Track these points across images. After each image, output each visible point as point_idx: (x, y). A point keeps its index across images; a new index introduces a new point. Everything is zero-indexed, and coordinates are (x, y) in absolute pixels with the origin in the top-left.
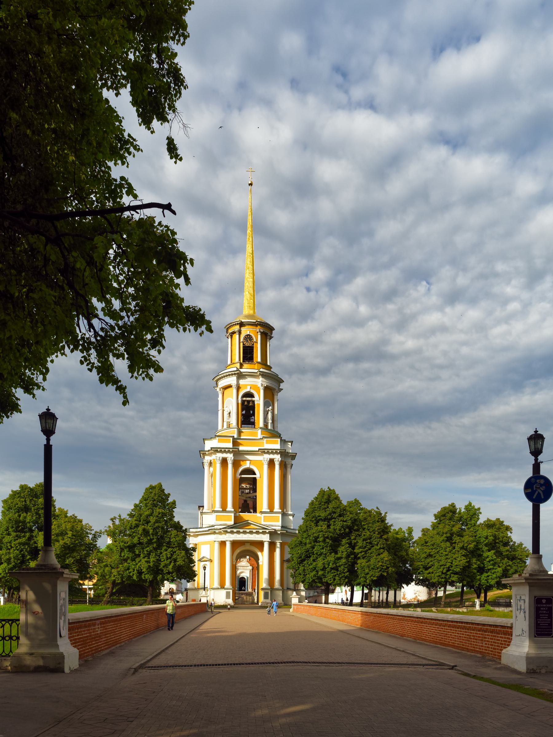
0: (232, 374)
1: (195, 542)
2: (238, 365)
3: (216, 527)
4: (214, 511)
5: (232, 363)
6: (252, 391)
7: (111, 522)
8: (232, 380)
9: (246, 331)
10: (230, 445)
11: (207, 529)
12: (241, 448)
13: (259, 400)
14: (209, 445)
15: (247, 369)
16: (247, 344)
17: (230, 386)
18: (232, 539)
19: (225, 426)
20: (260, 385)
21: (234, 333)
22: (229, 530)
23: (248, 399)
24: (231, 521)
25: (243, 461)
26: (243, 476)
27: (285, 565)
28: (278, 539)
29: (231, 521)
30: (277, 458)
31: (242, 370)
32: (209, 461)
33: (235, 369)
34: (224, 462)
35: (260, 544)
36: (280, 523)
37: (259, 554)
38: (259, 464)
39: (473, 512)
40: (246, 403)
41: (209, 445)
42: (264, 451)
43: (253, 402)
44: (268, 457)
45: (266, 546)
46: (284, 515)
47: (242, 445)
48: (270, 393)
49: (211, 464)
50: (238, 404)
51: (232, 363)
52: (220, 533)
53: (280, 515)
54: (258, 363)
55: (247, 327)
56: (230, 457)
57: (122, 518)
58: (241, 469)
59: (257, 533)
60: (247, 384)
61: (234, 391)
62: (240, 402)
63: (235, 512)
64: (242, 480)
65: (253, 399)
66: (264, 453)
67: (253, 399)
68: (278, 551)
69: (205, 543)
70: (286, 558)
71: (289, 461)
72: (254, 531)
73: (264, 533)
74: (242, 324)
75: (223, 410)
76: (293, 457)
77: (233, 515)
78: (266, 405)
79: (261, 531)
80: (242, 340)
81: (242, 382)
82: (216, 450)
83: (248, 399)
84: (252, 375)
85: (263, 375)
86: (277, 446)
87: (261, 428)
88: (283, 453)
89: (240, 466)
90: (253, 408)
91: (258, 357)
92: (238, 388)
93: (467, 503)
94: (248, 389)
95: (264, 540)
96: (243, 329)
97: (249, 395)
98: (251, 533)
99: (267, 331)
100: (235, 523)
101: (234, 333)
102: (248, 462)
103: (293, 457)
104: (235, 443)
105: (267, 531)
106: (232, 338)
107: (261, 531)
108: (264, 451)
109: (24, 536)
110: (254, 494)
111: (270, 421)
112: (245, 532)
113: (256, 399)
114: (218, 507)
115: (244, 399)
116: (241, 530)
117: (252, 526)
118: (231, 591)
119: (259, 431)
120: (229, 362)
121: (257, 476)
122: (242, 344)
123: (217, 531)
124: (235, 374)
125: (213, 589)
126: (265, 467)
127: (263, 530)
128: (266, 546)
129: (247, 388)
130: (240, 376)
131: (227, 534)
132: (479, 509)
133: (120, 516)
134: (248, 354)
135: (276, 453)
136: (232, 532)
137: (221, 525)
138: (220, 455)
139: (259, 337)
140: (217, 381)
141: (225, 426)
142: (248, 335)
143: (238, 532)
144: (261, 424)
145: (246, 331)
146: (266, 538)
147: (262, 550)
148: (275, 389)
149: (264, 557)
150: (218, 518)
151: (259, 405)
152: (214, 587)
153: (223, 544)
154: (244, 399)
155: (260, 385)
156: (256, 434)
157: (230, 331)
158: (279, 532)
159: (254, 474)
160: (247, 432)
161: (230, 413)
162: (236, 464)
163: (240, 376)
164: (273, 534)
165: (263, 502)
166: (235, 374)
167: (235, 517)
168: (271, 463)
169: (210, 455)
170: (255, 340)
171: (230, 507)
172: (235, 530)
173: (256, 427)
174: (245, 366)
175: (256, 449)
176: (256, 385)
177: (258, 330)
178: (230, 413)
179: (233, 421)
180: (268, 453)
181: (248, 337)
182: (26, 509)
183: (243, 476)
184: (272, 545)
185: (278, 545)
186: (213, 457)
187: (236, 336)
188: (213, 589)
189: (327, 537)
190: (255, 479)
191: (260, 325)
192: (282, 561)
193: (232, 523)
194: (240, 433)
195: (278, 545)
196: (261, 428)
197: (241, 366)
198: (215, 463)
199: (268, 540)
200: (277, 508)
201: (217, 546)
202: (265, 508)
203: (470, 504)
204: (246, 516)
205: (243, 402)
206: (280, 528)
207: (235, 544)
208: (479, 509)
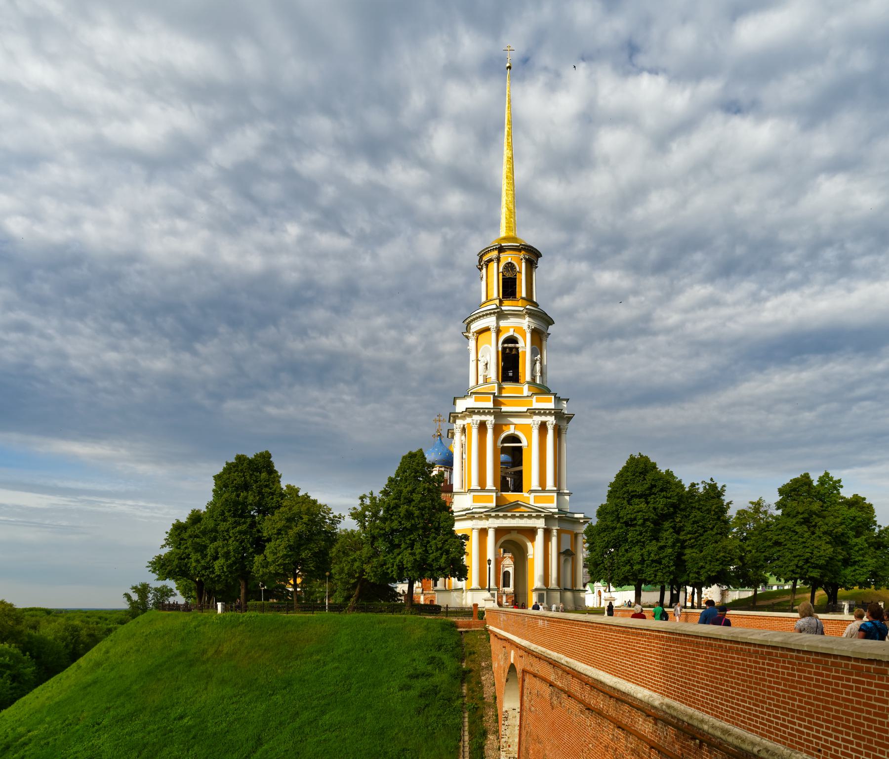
0: (491, 314)
2: (497, 302)
3: (474, 510)
4: (470, 491)
5: (488, 300)
6: (516, 335)
7: (360, 502)
8: (491, 321)
9: (506, 258)
10: (490, 405)
11: (464, 513)
12: (504, 409)
13: (525, 346)
14: (461, 406)
15: (507, 306)
16: (508, 275)
17: (487, 329)
18: (496, 526)
19: (481, 381)
20: (525, 327)
21: (491, 260)
22: (493, 514)
23: (510, 345)
25: (506, 425)
26: (506, 445)
27: (562, 558)
28: (554, 525)
30: (551, 420)
31: (503, 308)
33: (494, 307)
34: (482, 426)
35: (531, 533)
36: (555, 505)
37: (529, 544)
38: (527, 429)
39: (830, 486)
41: (461, 406)
42: (533, 412)
43: (517, 349)
44: (538, 419)
46: (559, 493)
47: (504, 404)
48: (538, 337)
49: (464, 430)
50: (498, 352)
51: (488, 300)
52: (480, 518)
53: (555, 494)
54: (522, 298)
55: (508, 252)
56: (490, 420)
57: (374, 495)
58: (503, 436)
59: (530, 517)
60: (510, 326)
61: (493, 335)
62: (500, 349)
63: (496, 491)
64: (504, 450)
66: (535, 414)
68: (554, 540)
70: (562, 550)
71: (563, 424)
72: (526, 514)
73: (538, 517)
74: (501, 249)
75: (477, 360)
76: (569, 418)
77: (494, 494)
78: (534, 352)
79: (534, 514)
80: (501, 270)
81: (503, 323)
82: (471, 412)
83: (510, 345)
84: (516, 314)
85: (531, 314)
86: (551, 405)
87: (528, 383)
88: (558, 414)
89: (503, 431)
90: (517, 356)
91: (522, 291)
92: (498, 331)
93: (822, 474)
94: (511, 333)
95: (537, 526)
96: (502, 255)
97: (512, 340)
98: (522, 517)
99: (533, 258)
100: (497, 506)
101: (491, 260)
102: (512, 427)
103: (569, 418)
104: (496, 402)
105: (543, 515)
106: (487, 268)
107: (534, 514)
108: (533, 412)
109: (244, 523)
110: (518, 469)
111: (538, 374)
112: (513, 517)
113: (521, 344)
114: (475, 485)
115: (506, 345)
116: (509, 514)
117: (522, 509)
119: (526, 387)
120: (484, 299)
121: (524, 443)
122: (501, 275)
123: (476, 516)
124: (494, 313)
125: (472, 590)
127: (537, 513)
129: (509, 331)
130: (501, 315)
131: (490, 520)
132: (839, 481)
133: (372, 494)
134: (509, 288)
135: (550, 414)
136: (497, 517)
138: (477, 418)
139: (524, 265)
140: (469, 324)
141: (481, 381)
143: (505, 517)
144: (528, 378)
145: (506, 258)
146: (540, 523)
147: (533, 539)
149: (535, 550)
150: (475, 499)
151: (524, 353)
152: (473, 587)
153: (483, 532)
154: (506, 345)
155: (525, 327)
156: (521, 391)
157: (485, 258)
158: (556, 516)
160: (509, 388)
162: (497, 429)
163: (501, 315)
164: (549, 518)
165: (531, 478)
166: (494, 313)
167: (497, 497)
168: (543, 427)
169: (464, 418)
171: (490, 484)
172: (501, 514)
173: (521, 381)
174: (506, 302)
175: (524, 409)
176: (520, 326)
177: (522, 256)
179: (492, 374)
180: (540, 414)
181: (510, 266)
182: (246, 487)
183: (506, 445)
184: (547, 532)
185: (555, 532)
186: (468, 420)
187: (494, 265)
188: (472, 590)
189: (647, 520)
190: (520, 449)
191: (524, 249)
192: (559, 554)
193: (493, 505)
194: (500, 389)
195: (555, 532)
196: (528, 383)
197: (501, 302)
198: (470, 428)
199: (543, 525)
200: (550, 484)
202: (535, 484)
203: (827, 474)
204: (511, 496)
205: (504, 349)
206: (556, 510)
207: (499, 531)
208: (839, 481)
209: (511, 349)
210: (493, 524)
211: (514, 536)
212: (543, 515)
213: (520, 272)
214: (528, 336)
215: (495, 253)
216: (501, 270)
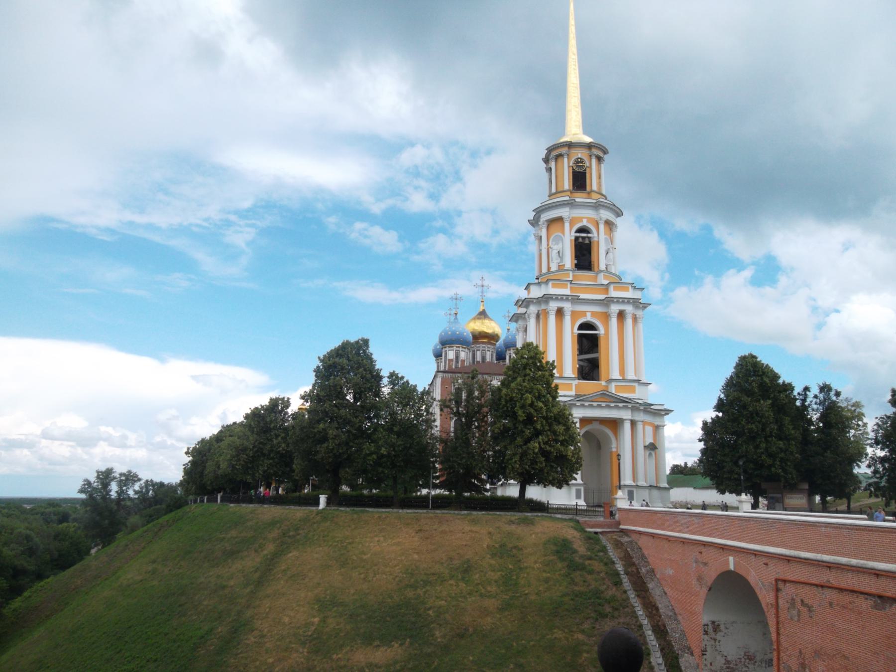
18: (581, 416)
24: (571, 390)
29: (571, 390)
40: (580, 240)
45: (627, 426)
65: (589, 235)
67: (589, 235)
94: (585, 223)
95: (624, 417)
118: (582, 489)
121: (601, 331)
126: (614, 321)
128: (627, 426)
162: (574, 315)
170: (588, 164)
172: (587, 404)
181: (579, 161)
202: (615, 375)
205: (577, 238)
209: (583, 238)
211: (595, 426)
212: (630, 405)
213: (590, 167)
215: (564, 150)
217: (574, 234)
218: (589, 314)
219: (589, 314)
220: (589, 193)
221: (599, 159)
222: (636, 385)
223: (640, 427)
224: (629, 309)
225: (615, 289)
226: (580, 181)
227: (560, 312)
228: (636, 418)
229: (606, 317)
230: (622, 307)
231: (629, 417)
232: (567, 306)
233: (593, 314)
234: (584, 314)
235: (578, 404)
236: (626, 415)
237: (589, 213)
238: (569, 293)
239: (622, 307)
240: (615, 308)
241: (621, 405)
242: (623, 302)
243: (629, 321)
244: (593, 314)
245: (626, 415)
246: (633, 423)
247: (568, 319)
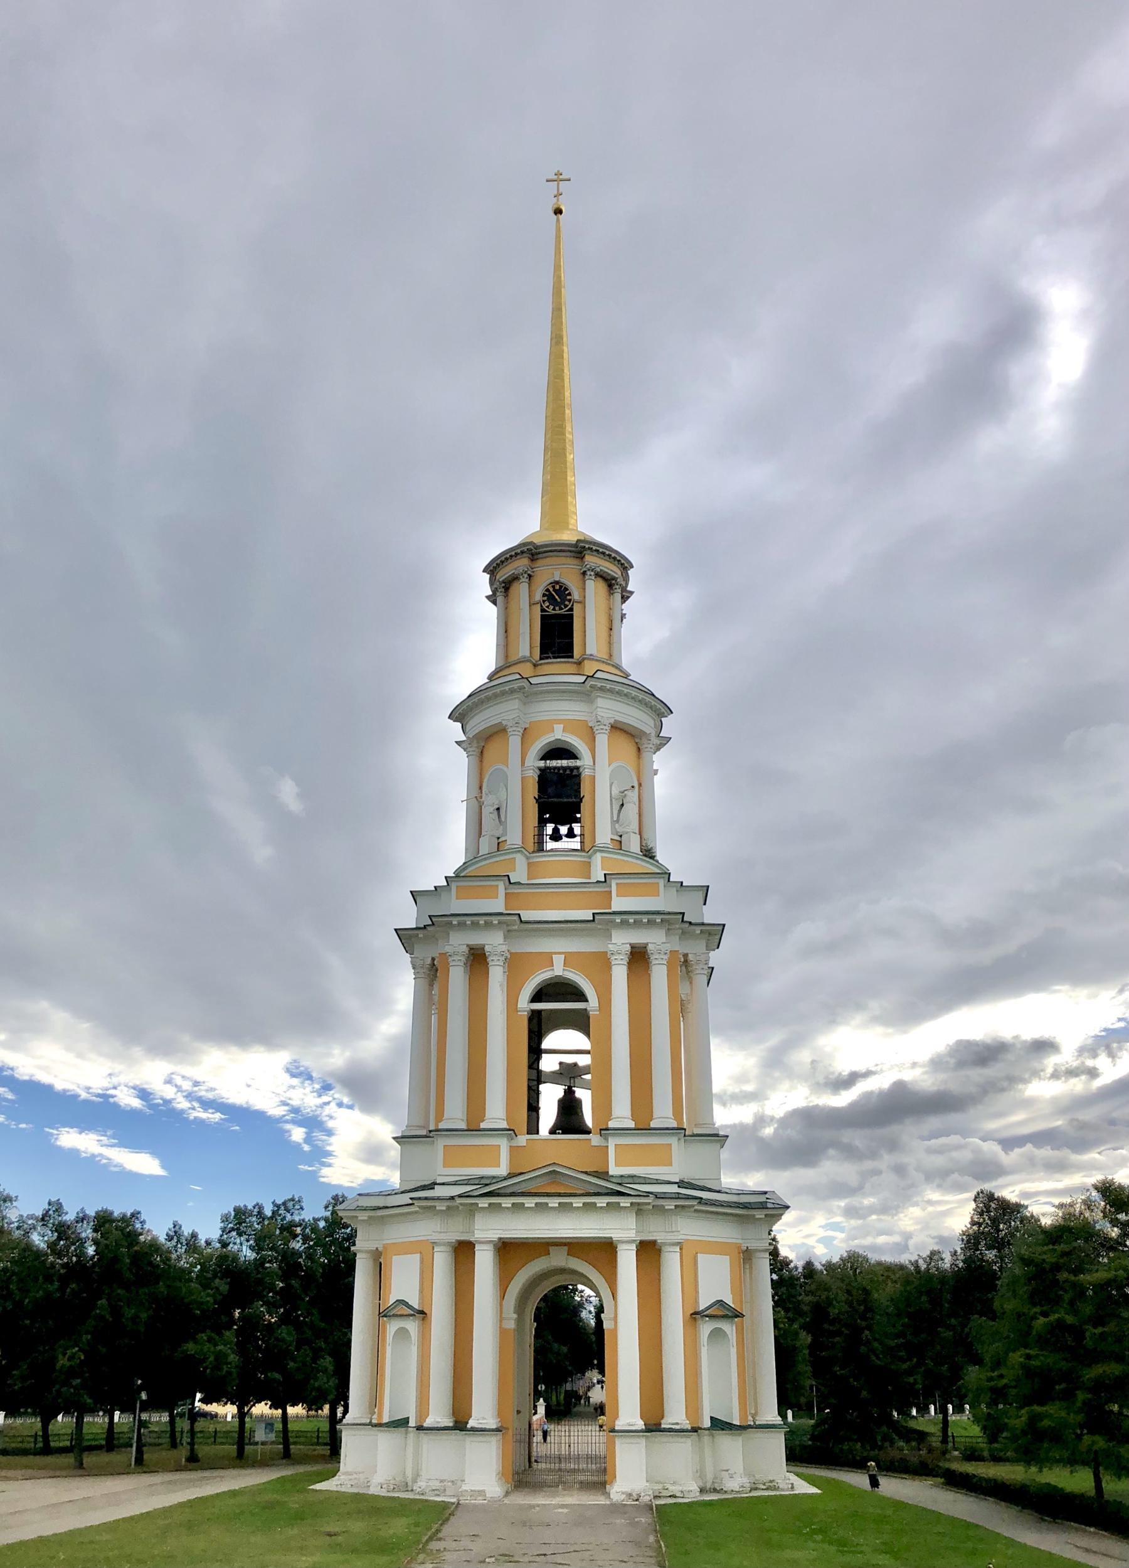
1: (373, 1246)
3: (439, 1191)
9: (550, 572)
18: (495, 1235)
21: (515, 578)
32: (429, 961)
35: (603, 1252)
61: (515, 741)
69: (407, 1248)
95: (615, 1235)
101: (515, 578)
106: (506, 596)
113: (585, 762)
126: (620, 974)
137: (455, 1183)
142: (557, 582)
148: (642, 734)
159: (581, 996)
161: (498, 809)
162: (516, 965)
170: (576, 596)
178: (498, 809)
187: (521, 590)
201: (442, 1261)
210: (489, 1229)
212: (625, 1202)
213: (582, 602)
214: (602, 740)
215: (522, 563)
216: (538, 597)
217: (534, 763)
218: (558, 961)
219: (558, 961)
220: (579, 663)
221: (610, 583)
222: (673, 1141)
223: (672, 1264)
224: (655, 940)
225: (623, 892)
226: (557, 636)
227: (477, 958)
228: (660, 1237)
229: (601, 964)
230: (638, 937)
231: (632, 1235)
232: (494, 942)
233: (570, 959)
234: (547, 959)
235: (484, 1203)
236: (622, 1229)
237: (573, 710)
238: (502, 910)
239: (638, 937)
240: (621, 941)
241: (602, 1202)
242: (637, 924)
243: (659, 975)
244: (570, 959)
245: (622, 1229)
246: (649, 1251)
247: (497, 975)
